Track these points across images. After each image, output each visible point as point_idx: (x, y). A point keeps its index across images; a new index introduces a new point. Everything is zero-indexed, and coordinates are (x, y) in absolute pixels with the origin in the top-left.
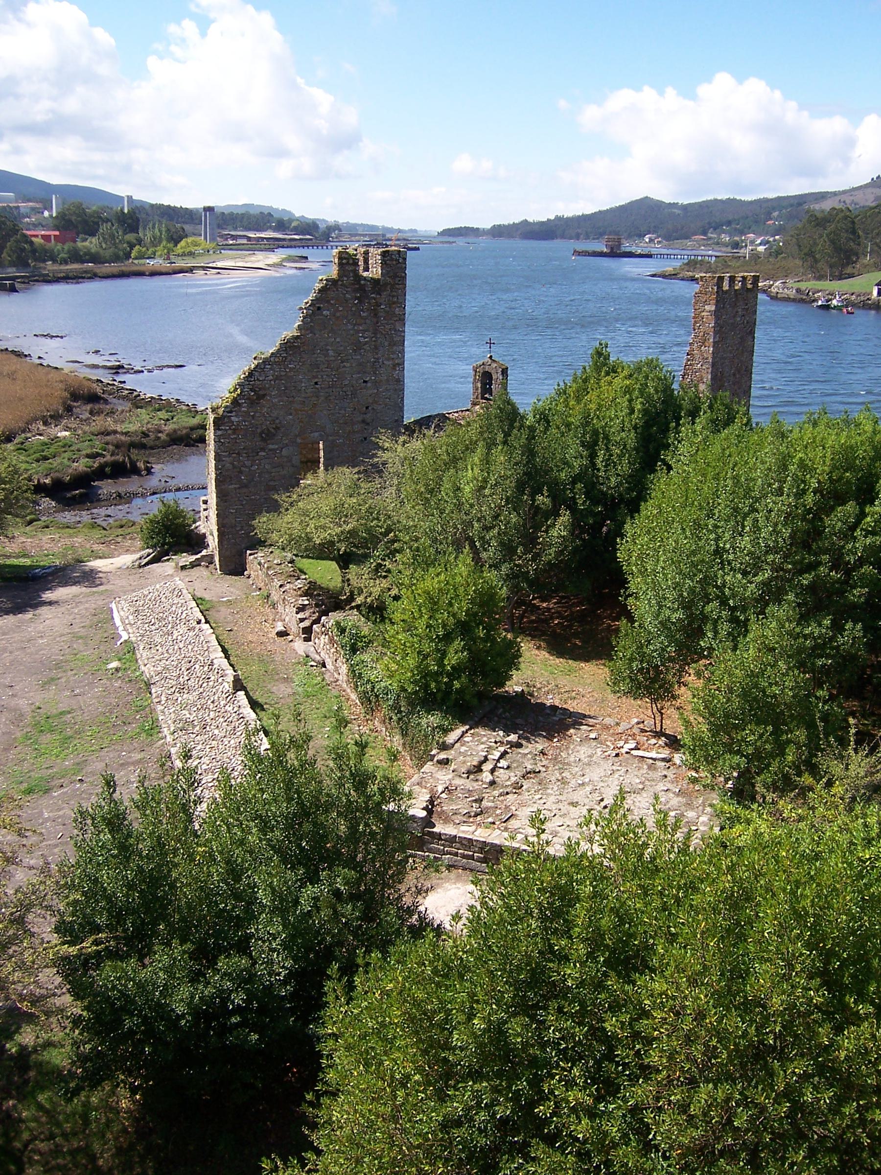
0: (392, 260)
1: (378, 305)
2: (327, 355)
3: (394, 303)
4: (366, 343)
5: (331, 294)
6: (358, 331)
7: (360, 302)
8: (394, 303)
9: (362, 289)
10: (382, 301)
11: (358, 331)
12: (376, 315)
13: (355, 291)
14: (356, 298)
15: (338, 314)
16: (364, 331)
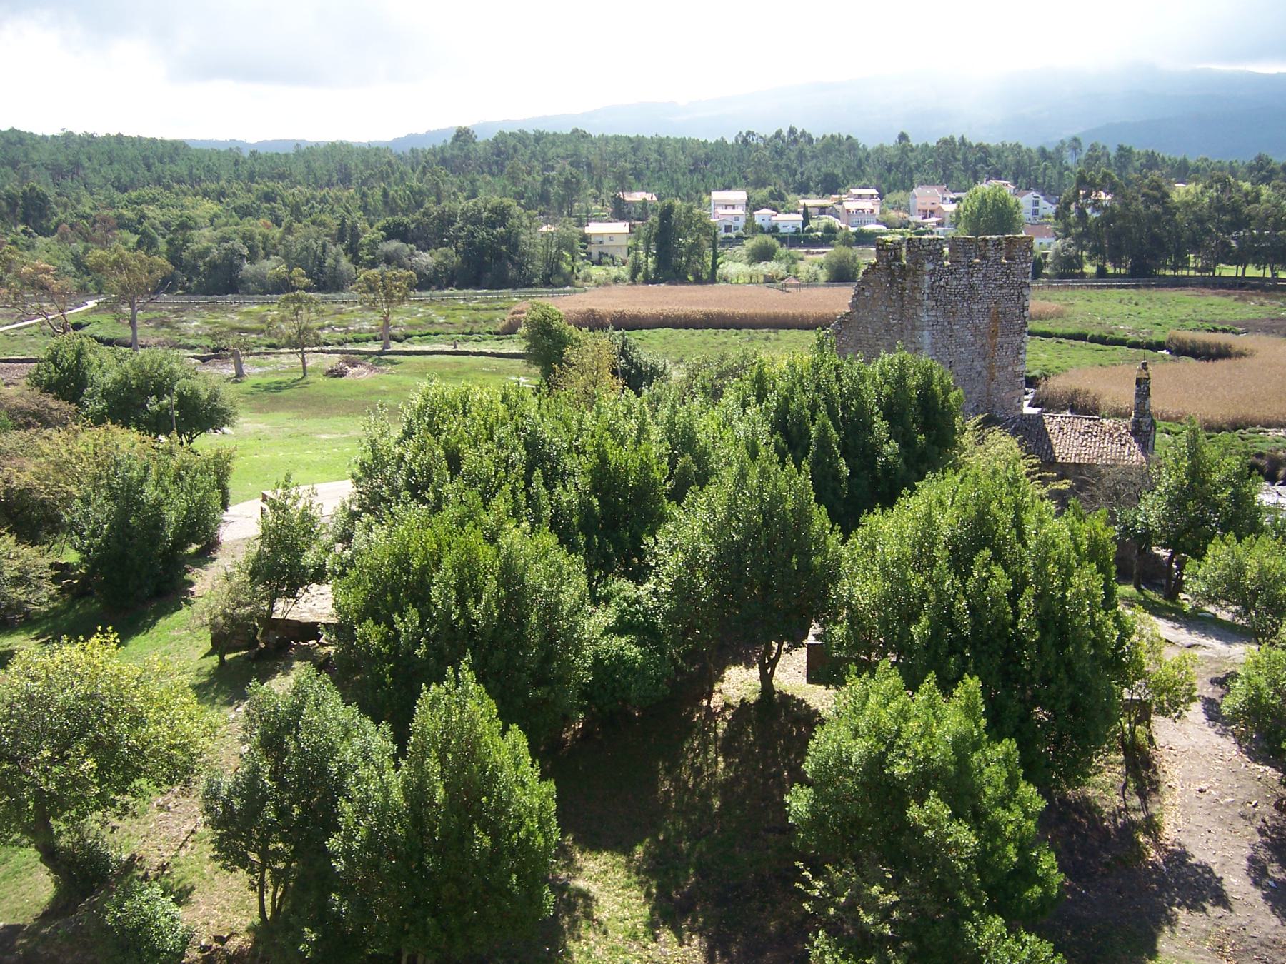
0: (914, 246)
1: (904, 289)
2: (867, 332)
3: (916, 288)
4: (894, 325)
5: (871, 276)
6: (889, 313)
7: (891, 286)
8: (916, 288)
9: (892, 273)
10: (906, 286)
11: (889, 313)
12: (902, 300)
13: (888, 275)
14: (889, 282)
15: (875, 296)
16: (894, 313)
